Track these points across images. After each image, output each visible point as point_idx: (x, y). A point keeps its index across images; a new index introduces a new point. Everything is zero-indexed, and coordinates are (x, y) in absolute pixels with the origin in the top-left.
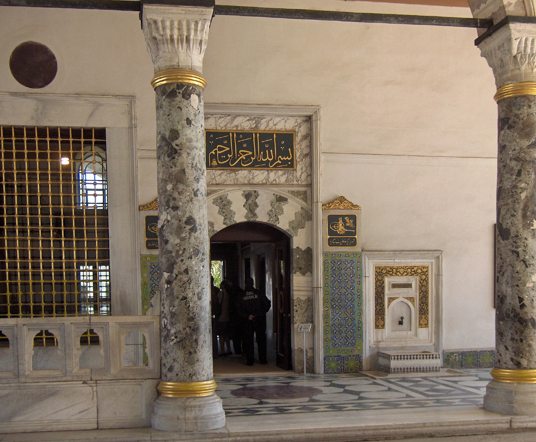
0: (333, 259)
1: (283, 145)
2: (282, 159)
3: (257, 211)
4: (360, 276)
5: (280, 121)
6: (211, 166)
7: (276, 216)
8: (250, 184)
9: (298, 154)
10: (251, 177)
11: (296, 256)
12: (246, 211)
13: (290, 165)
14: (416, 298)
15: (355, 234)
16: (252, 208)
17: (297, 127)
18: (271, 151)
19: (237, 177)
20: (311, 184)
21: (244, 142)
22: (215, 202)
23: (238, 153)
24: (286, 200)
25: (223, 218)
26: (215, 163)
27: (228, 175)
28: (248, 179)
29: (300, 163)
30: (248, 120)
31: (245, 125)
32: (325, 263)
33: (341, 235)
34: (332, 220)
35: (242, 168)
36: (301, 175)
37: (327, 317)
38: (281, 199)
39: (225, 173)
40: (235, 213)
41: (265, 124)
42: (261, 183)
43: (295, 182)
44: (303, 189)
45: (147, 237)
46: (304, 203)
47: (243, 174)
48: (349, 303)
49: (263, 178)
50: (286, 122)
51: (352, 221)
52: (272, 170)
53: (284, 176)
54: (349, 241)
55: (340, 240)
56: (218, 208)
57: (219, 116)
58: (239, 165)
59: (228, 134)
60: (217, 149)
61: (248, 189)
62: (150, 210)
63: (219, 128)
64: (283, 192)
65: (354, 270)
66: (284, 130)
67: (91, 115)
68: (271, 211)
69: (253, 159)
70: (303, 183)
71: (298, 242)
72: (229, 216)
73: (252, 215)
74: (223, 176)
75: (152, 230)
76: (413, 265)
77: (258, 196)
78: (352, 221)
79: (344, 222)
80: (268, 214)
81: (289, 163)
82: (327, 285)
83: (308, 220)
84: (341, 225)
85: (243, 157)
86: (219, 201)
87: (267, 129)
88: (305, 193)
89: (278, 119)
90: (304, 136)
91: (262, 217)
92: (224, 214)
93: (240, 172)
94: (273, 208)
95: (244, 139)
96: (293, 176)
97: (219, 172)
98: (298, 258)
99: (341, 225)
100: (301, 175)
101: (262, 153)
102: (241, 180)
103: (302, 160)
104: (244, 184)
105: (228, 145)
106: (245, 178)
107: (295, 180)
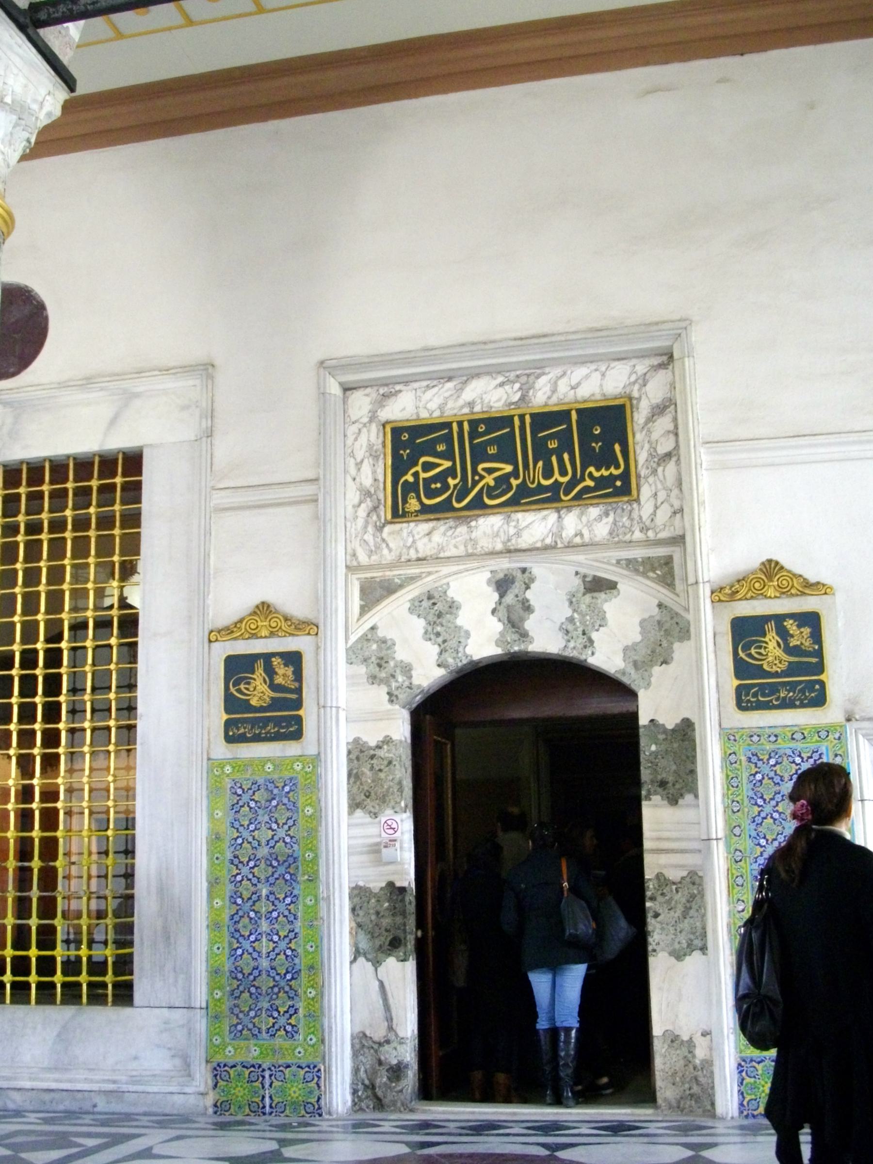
0: (754, 748)
1: (597, 439)
2: (597, 474)
3: (530, 624)
5: (587, 377)
6: (405, 514)
7: (584, 634)
8: (509, 551)
9: (641, 456)
10: (512, 531)
11: (648, 748)
12: (500, 627)
13: (620, 488)
15: (820, 668)
16: (515, 618)
17: (636, 387)
18: (566, 456)
19: (473, 535)
20: (683, 537)
21: (490, 442)
22: (415, 607)
23: (475, 472)
24: (611, 586)
25: (436, 649)
26: (413, 504)
27: (450, 533)
28: (503, 537)
29: (651, 480)
30: (502, 385)
31: (494, 399)
32: (729, 759)
33: (776, 675)
34: (746, 631)
35: (489, 511)
36: (654, 513)
38: (598, 586)
39: (442, 529)
40: (468, 634)
41: (547, 389)
42: (539, 545)
43: (638, 535)
44: (661, 552)
45: (227, 710)
46: (664, 594)
47: (490, 527)
49: (546, 532)
50: (603, 375)
51: (807, 631)
52: (569, 508)
53: (605, 520)
54: (802, 691)
55: (774, 689)
57: (425, 383)
58: (478, 504)
59: (448, 425)
60: (419, 468)
61: (504, 565)
62: (235, 639)
63: (424, 414)
66: (598, 397)
67: (113, 421)
68: (571, 620)
69: (514, 482)
70: (663, 535)
71: (655, 706)
72: (453, 643)
73: (516, 637)
74: (437, 538)
75: (239, 691)
77: (532, 580)
78: (807, 631)
79: (783, 633)
80: (561, 628)
81: (618, 483)
82: (737, 831)
83: (681, 639)
84: (772, 645)
85: (490, 480)
86: (426, 604)
87: (554, 400)
88: (668, 561)
89: (579, 373)
90: (658, 406)
91: (545, 639)
92: (440, 640)
93: (481, 520)
94: (574, 611)
95: (491, 435)
97: (425, 527)
98: (655, 754)
99: (772, 645)
100: (654, 513)
101: (540, 464)
102: (486, 544)
103: (654, 472)
104: (493, 554)
105: (448, 455)
106: (497, 535)
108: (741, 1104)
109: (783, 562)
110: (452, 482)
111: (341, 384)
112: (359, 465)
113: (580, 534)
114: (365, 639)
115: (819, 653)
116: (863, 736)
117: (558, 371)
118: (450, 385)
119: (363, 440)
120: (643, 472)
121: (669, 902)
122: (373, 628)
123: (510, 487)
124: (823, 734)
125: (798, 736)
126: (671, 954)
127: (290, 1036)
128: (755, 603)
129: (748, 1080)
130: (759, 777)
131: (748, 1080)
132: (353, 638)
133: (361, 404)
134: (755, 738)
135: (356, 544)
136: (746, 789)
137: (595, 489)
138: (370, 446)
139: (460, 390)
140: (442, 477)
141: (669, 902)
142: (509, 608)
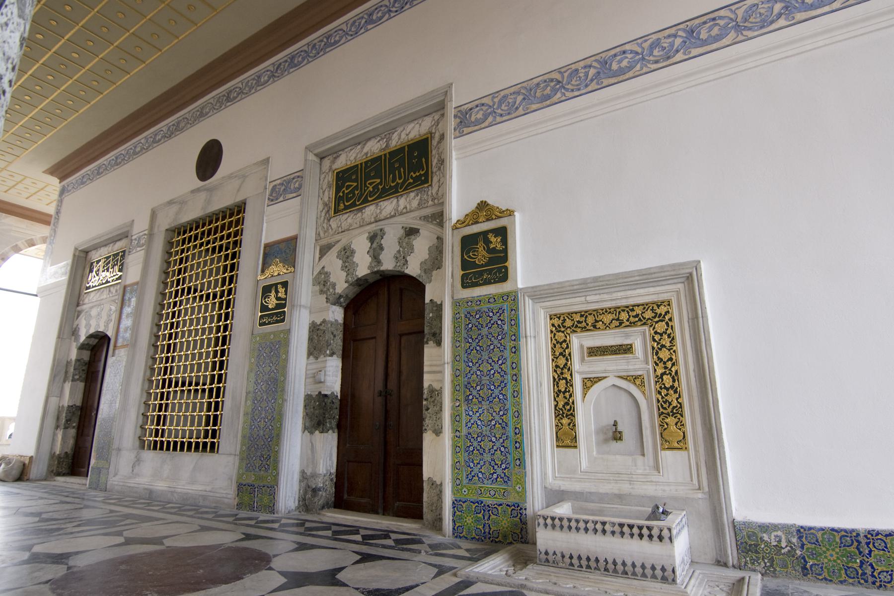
0: (469, 309)
4: (516, 337)
6: (339, 211)
10: (378, 211)
12: (370, 259)
14: (649, 376)
15: (505, 259)
21: (371, 170)
23: (365, 185)
26: (342, 206)
28: (375, 215)
33: (482, 266)
34: (468, 243)
37: (458, 418)
43: (430, 203)
48: (497, 392)
55: (481, 274)
56: (340, 262)
58: (366, 201)
61: (373, 228)
64: (410, 220)
65: (505, 327)
68: (399, 251)
69: (380, 187)
72: (351, 270)
74: (349, 220)
76: (631, 302)
77: (384, 234)
91: (388, 264)
96: (428, 195)
102: (367, 220)
105: (356, 180)
107: (430, 199)
108: (454, 529)
109: (489, 202)
110: (356, 192)
111: (315, 155)
112: (324, 192)
113: (406, 208)
114: (320, 273)
115: (505, 251)
116: (529, 296)
117: (402, 128)
118: (359, 147)
119: (326, 181)
120: (434, 170)
121: (433, 402)
122: (323, 268)
123: (378, 189)
124: (505, 298)
125: (492, 300)
126: (434, 432)
127: (266, 470)
128: (474, 226)
129: (458, 513)
130: (470, 326)
131: (458, 513)
132: (315, 273)
133: (327, 162)
134: (470, 304)
135: (320, 229)
136: (464, 333)
137: (414, 182)
138: (329, 182)
139: (363, 148)
140: (352, 192)
141: (433, 402)
142: (374, 249)
